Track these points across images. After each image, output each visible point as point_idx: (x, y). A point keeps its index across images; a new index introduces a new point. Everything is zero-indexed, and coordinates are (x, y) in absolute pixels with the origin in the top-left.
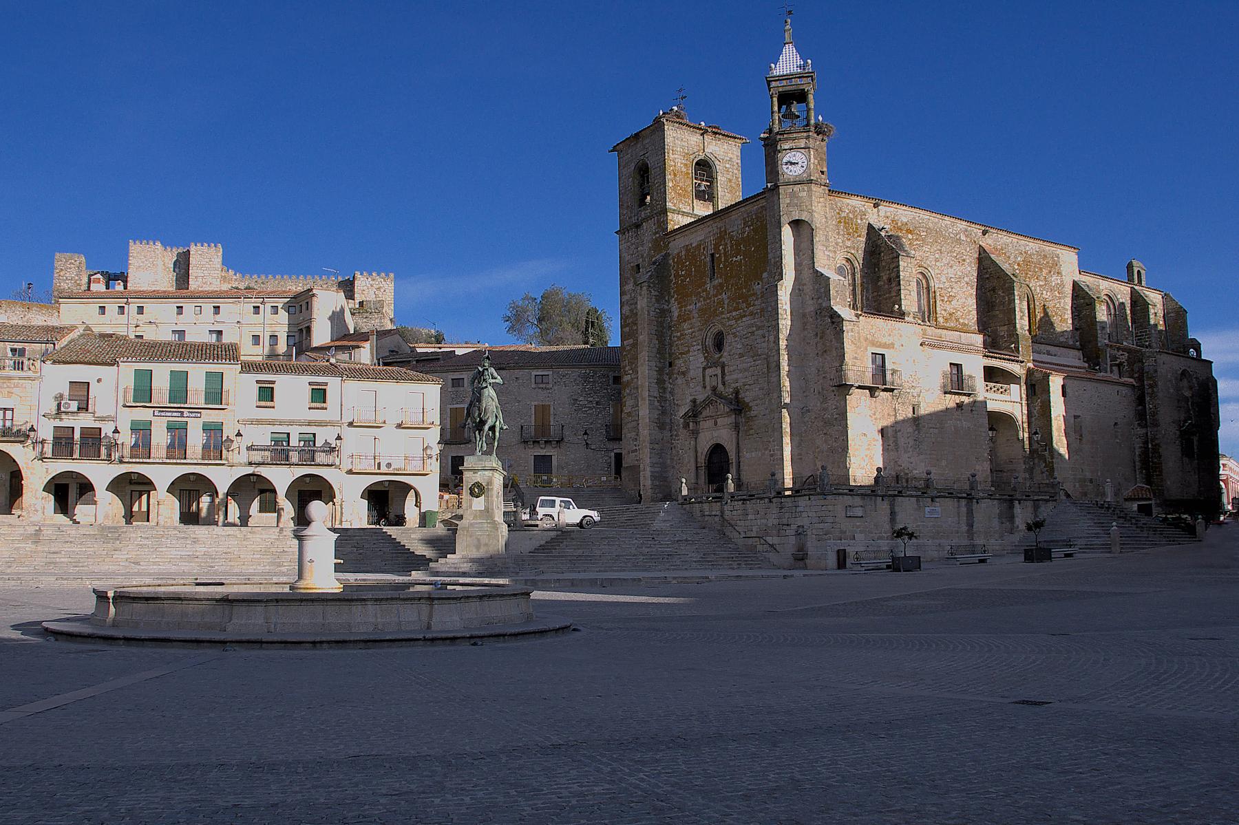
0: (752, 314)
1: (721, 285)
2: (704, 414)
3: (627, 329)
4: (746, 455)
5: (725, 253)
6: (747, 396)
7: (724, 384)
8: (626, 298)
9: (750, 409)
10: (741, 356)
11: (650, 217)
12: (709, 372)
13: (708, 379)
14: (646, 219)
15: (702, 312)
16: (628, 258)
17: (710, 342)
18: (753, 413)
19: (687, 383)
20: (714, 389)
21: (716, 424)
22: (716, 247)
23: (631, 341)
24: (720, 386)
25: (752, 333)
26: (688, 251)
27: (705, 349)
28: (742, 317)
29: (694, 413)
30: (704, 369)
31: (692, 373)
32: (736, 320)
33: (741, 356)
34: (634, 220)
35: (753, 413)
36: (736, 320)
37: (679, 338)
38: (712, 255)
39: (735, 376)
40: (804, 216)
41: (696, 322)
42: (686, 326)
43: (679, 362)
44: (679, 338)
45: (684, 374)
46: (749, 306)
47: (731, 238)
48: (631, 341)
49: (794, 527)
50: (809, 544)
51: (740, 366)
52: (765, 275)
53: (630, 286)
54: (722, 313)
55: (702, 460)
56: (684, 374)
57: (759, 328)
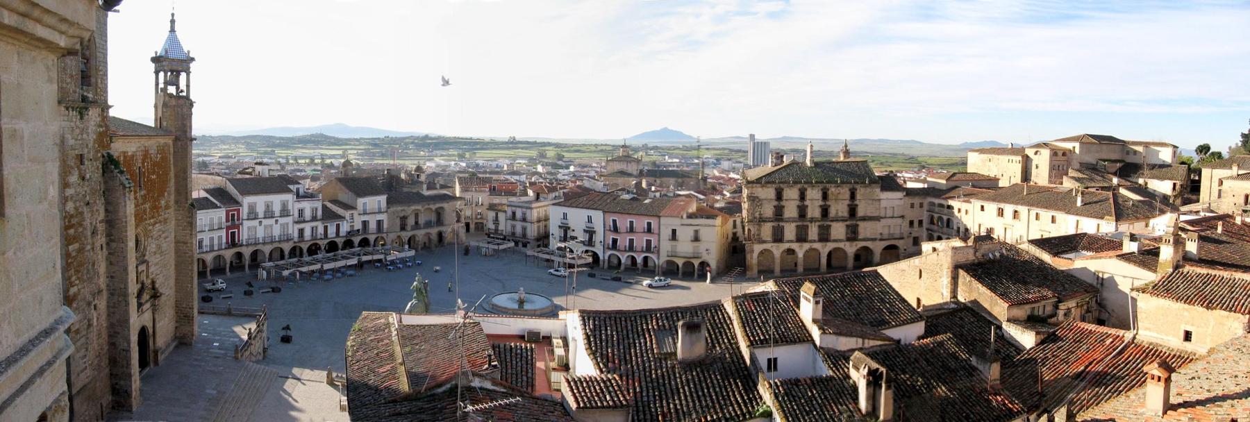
3: (72, 231)
23: (76, 246)
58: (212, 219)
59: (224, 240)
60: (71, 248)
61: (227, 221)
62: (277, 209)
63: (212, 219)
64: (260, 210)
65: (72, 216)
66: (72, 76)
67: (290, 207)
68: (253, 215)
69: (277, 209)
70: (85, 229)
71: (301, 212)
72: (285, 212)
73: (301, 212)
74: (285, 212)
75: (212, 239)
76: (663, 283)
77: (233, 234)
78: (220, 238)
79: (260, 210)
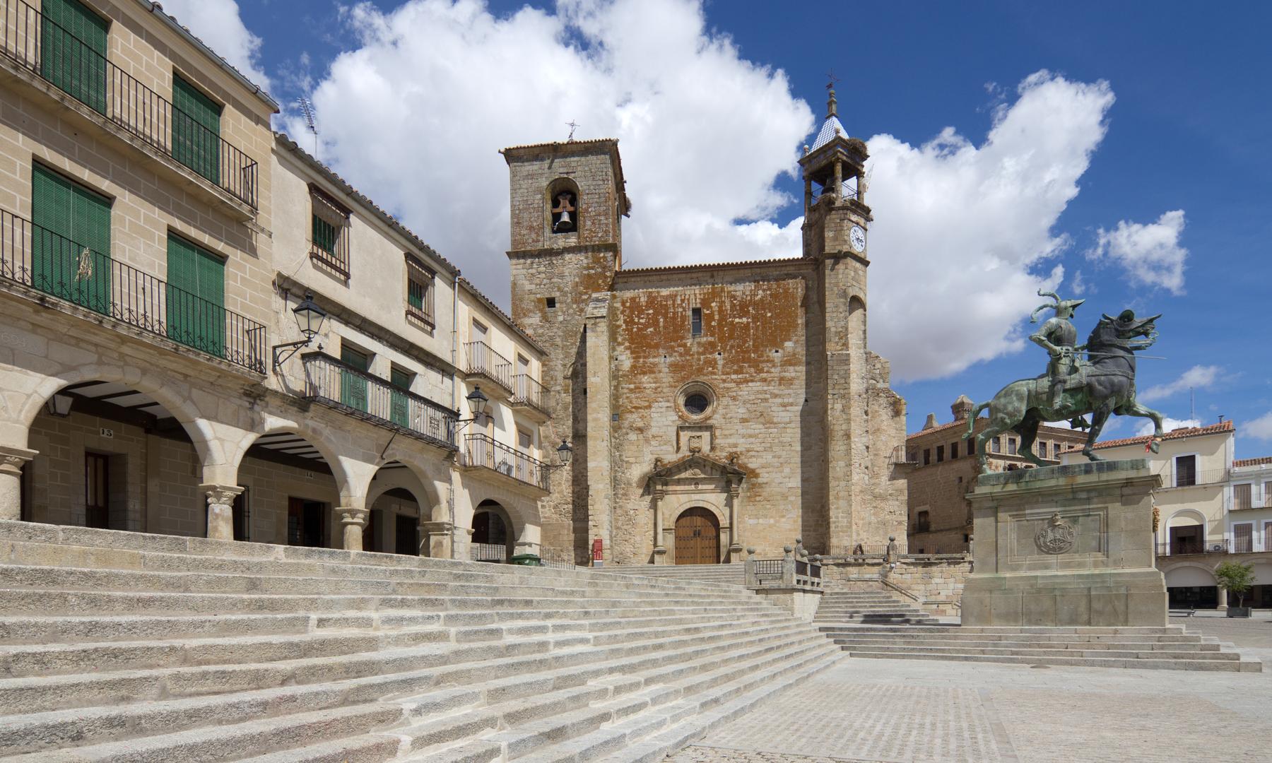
0: (764, 380)
1: (712, 345)
5: (721, 311)
10: (744, 421)
12: (681, 433)
15: (675, 368)
17: (681, 401)
19: (647, 441)
22: (706, 302)
24: (706, 448)
25: (766, 400)
27: (676, 408)
28: (746, 381)
29: (658, 480)
30: (681, 428)
31: (654, 431)
32: (738, 383)
33: (744, 421)
36: (738, 383)
37: (631, 390)
38: (697, 312)
39: (731, 441)
41: (666, 377)
42: (645, 379)
43: (633, 418)
45: (641, 430)
46: (761, 371)
51: (741, 431)
52: (788, 344)
54: (714, 374)
56: (641, 430)
57: (776, 396)
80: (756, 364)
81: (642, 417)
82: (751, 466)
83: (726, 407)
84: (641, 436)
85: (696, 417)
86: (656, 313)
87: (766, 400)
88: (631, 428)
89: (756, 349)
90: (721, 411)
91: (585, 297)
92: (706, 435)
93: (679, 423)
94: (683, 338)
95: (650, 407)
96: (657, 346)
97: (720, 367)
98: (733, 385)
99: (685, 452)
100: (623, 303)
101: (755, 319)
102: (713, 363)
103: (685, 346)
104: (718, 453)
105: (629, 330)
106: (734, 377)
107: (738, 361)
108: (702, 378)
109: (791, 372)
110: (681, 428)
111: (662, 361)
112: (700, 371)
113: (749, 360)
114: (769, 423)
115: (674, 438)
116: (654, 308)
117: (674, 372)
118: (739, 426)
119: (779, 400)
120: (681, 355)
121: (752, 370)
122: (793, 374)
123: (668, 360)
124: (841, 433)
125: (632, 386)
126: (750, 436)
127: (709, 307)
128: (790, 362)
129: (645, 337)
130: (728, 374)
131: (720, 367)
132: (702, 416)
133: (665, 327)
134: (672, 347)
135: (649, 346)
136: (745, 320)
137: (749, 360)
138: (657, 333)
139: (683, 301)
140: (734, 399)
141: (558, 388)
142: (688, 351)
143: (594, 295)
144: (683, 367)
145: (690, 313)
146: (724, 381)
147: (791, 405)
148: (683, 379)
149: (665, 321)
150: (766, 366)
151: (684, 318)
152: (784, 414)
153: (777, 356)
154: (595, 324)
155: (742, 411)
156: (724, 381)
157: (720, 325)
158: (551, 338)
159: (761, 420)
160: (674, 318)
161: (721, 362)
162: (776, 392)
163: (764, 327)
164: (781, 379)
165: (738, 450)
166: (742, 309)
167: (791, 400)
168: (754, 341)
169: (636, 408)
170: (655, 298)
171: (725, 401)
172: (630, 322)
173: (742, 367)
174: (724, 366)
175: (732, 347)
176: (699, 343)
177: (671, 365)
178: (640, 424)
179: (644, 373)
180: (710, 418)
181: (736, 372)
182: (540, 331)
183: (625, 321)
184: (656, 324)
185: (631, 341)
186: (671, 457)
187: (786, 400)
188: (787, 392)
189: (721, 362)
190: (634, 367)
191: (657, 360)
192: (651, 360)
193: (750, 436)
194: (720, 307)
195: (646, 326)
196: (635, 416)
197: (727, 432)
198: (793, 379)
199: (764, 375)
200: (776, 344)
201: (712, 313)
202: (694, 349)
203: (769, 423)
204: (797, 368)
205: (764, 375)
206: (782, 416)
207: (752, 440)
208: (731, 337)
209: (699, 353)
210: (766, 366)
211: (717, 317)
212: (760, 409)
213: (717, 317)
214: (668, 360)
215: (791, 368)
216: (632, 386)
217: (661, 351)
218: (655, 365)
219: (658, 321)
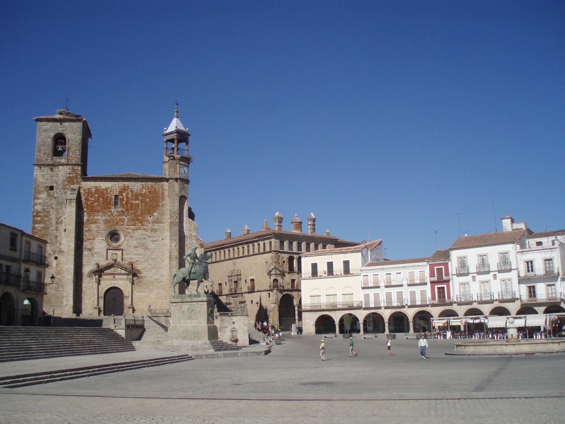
0: (145, 229)
1: (123, 212)
2: (105, 272)
3: (39, 218)
4: (136, 294)
5: (127, 197)
6: (139, 267)
7: (122, 260)
8: (37, 201)
9: (141, 273)
10: (136, 247)
11: (66, 165)
13: (109, 255)
14: (63, 165)
15: (106, 222)
16: (42, 180)
18: (142, 275)
19: (92, 255)
20: (115, 261)
21: (114, 277)
22: (121, 193)
23: (42, 225)
25: (145, 238)
26: (96, 189)
27: (106, 240)
28: (137, 229)
31: (96, 250)
33: (136, 247)
34: (50, 162)
35: (142, 275)
36: (134, 230)
37: (86, 231)
38: (116, 196)
39: (130, 256)
40: (186, 195)
41: (102, 225)
42: (93, 226)
44: (86, 231)
45: (90, 250)
46: (144, 225)
47: (133, 192)
48: (42, 225)
49: (229, 328)
50: (238, 335)
51: (135, 252)
52: (155, 214)
53: (44, 195)
54: (123, 225)
55: (102, 294)
56: (90, 250)
57: (150, 237)
58: (412, 274)
59: (429, 295)
60: (36, 225)
61: (432, 275)
62: (494, 262)
63: (412, 274)
64: (473, 265)
65: (40, 212)
66: (45, 154)
67: (512, 257)
68: (463, 271)
69: (494, 262)
70: (50, 219)
71: (530, 265)
72: (505, 266)
73: (530, 265)
74: (505, 266)
75: (413, 294)
76: (180, 300)
77: (441, 290)
78: (423, 293)
79: (473, 265)
80: (141, 222)
81: (91, 244)
82: (138, 268)
83: (128, 241)
84: (89, 253)
85: (115, 245)
86: (99, 196)
87: (145, 238)
88: (86, 249)
89: (142, 214)
90: (126, 243)
91: (67, 187)
92: (119, 253)
93: (107, 247)
94: (110, 208)
95: (94, 239)
96: (98, 211)
97: (126, 222)
98: (131, 231)
99: (110, 261)
100: (85, 191)
101: (142, 202)
102: (123, 220)
103: (111, 212)
104: (124, 262)
105: (87, 204)
106: (132, 227)
107: (134, 220)
108: (117, 228)
109: (156, 226)
110: (108, 249)
111: (100, 218)
112: (117, 223)
113: (138, 220)
114: (146, 249)
115: (105, 254)
116: (98, 194)
117: (106, 223)
118: (133, 250)
119: (151, 239)
120: (109, 216)
121: (140, 224)
122: (157, 227)
123: (104, 218)
124: (174, 256)
125: (87, 229)
126: (138, 254)
127: (122, 195)
128: (157, 221)
129: (93, 207)
130: (129, 225)
131: (126, 222)
132: (117, 244)
133: (103, 203)
134: (105, 212)
135: (95, 211)
136: (137, 202)
137: (138, 220)
138: (99, 205)
139: (111, 191)
140: (132, 237)
141: (53, 228)
142: (112, 214)
143: (72, 186)
144: (110, 221)
145: (113, 197)
146: (128, 229)
147: (156, 241)
148: (110, 227)
149: (103, 200)
150: (145, 223)
151: (111, 199)
152: (153, 245)
153: (150, 219)
154: (71, 202)
155: (135, 243)
156: (128, 229)
157: (127, 203)
158: (51, 204)
159: (143, 247)
160: (107, 199)
161: (126, 220)
162: (150, 235)
163: (145, 206)
164: (152, 229)
165: (133, 261)
166: (136, 197)
167: (156, 239)
168: (141, 211)
169: (88, 239)
170: (99, 189)
171: (128, 238)
172: (87, 199)
173: (135, 223)
174: (128, 222)
175: (131, 213)
176: (117, 211)
177: (105, 220)
178: (89, 247)
179: (92, 223)
180: (121, 245)
181: (133, 225)
182: (46, 201)
183: (85, 199)
184: (98, 201)
185: (87, 207)
186: (103, 263)
187: (154, 239)
188: (154, 235)
189: (126, 220)
190: (88, 220)
191: (98, 217)
192: (96, 217)
193: (138, 254)
194: (127, 196)
195: (94, 202)
196: (87, 243)
197: (128, 252)
198: (157, 229)
199: (145, 227)
200: (150, 213)
201: (123, 197)
202: (115, 214)
203: (146, 249)
204: (159, 225)
205: (145, 227)
206: (152, 246)
207: (139, 256)
208: (131, 209)
209: (117, 216)
210: (145, 223)
211: (125, 200)
212: (143, 242)
213: (125, 200)
214: (104, 218)
215: (157, 224)
216: (87, 229)
217: (100, 214)
218: (97, 220)
219: (99, 199)
